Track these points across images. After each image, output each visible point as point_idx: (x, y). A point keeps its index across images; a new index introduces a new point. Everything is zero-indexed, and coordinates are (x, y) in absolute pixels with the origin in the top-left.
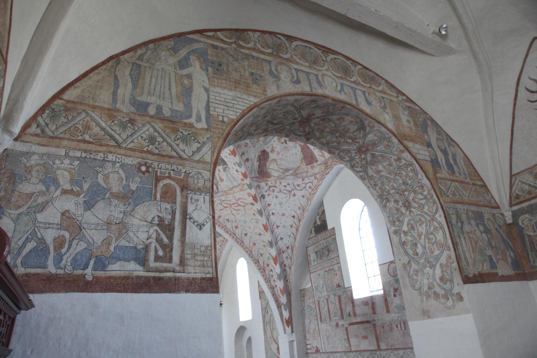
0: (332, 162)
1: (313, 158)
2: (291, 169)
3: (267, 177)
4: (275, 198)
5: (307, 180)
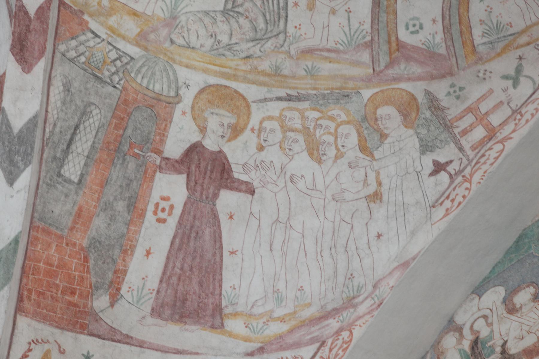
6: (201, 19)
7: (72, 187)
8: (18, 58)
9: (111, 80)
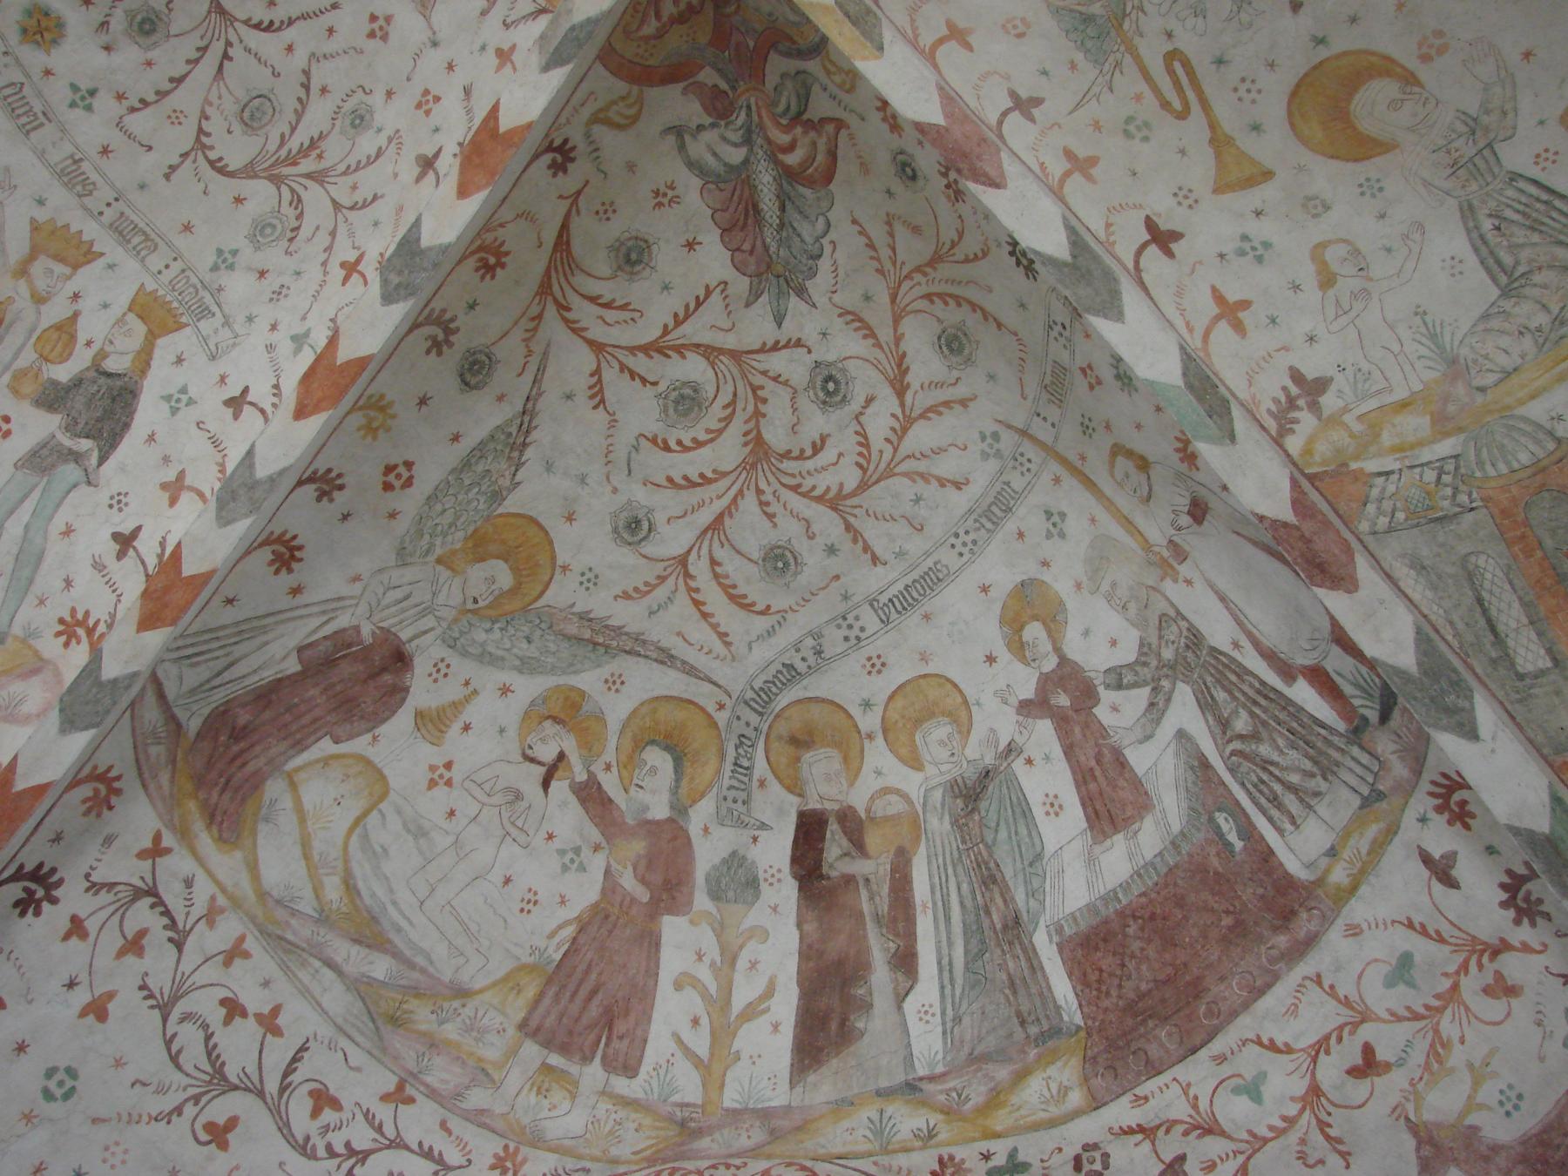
0: (755, 1152)
1: (621, 1027)
2: (396, 954)
3: (212, 816)
4: (82, 997)
5: (419, 1121)
6: (1486, 330)
7: (1552, 677)
8: (1328, 584)
9: (1459, 505)
